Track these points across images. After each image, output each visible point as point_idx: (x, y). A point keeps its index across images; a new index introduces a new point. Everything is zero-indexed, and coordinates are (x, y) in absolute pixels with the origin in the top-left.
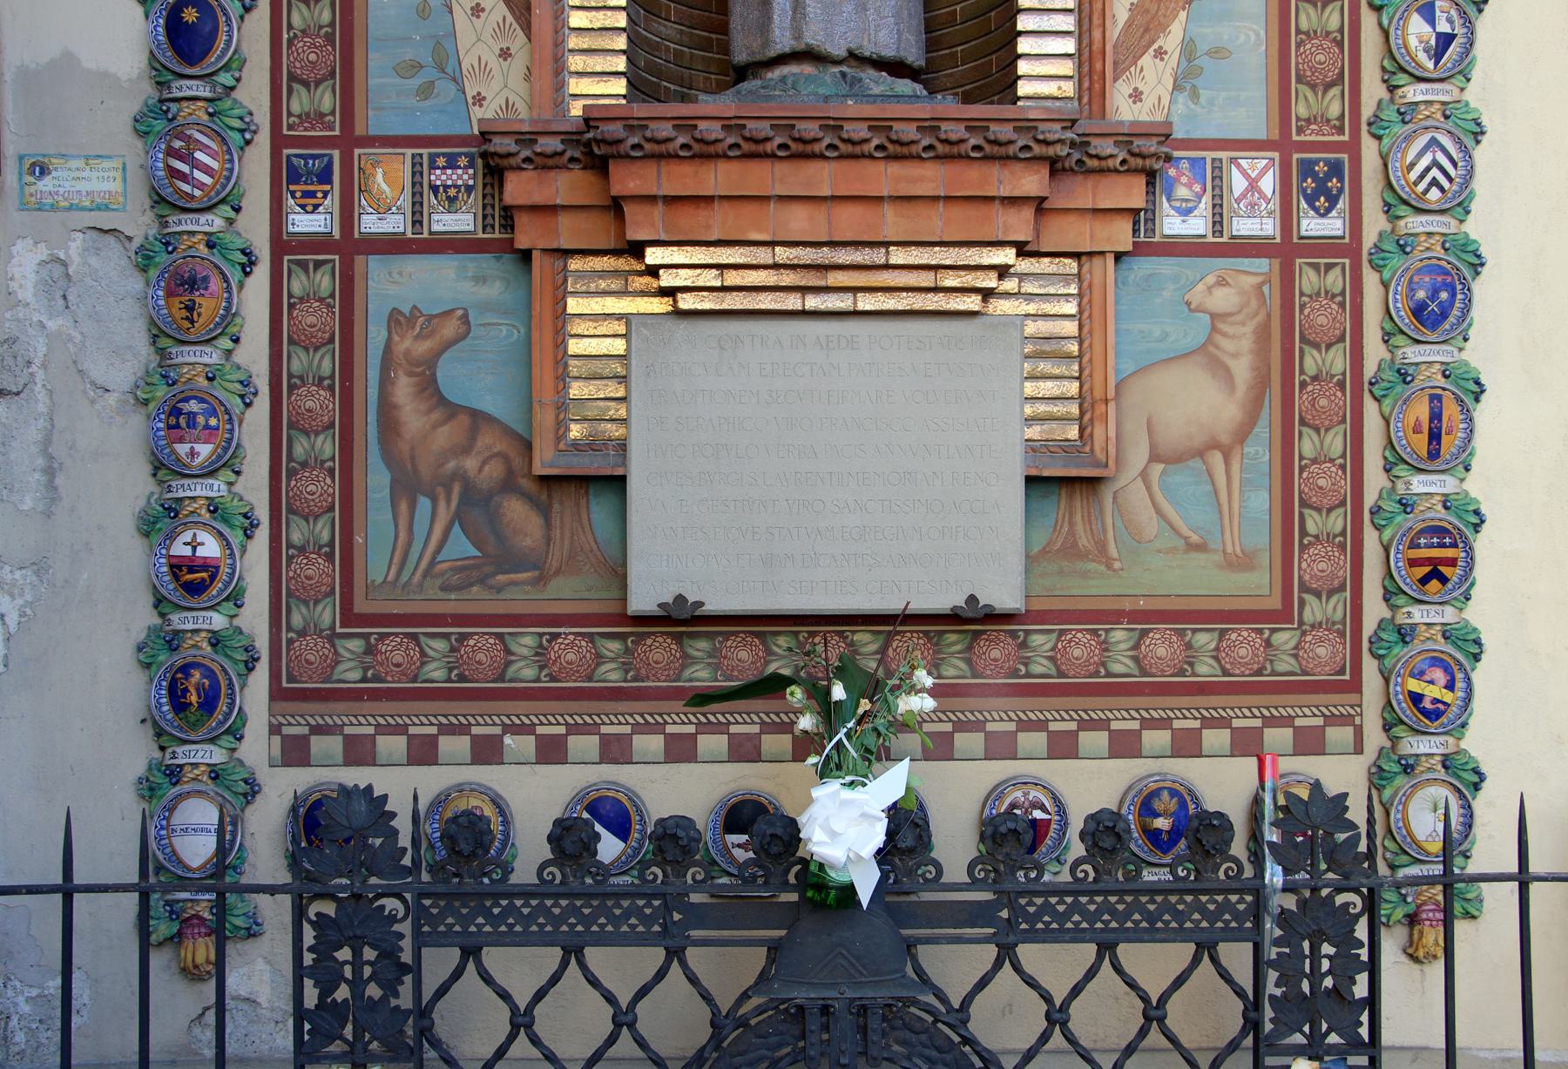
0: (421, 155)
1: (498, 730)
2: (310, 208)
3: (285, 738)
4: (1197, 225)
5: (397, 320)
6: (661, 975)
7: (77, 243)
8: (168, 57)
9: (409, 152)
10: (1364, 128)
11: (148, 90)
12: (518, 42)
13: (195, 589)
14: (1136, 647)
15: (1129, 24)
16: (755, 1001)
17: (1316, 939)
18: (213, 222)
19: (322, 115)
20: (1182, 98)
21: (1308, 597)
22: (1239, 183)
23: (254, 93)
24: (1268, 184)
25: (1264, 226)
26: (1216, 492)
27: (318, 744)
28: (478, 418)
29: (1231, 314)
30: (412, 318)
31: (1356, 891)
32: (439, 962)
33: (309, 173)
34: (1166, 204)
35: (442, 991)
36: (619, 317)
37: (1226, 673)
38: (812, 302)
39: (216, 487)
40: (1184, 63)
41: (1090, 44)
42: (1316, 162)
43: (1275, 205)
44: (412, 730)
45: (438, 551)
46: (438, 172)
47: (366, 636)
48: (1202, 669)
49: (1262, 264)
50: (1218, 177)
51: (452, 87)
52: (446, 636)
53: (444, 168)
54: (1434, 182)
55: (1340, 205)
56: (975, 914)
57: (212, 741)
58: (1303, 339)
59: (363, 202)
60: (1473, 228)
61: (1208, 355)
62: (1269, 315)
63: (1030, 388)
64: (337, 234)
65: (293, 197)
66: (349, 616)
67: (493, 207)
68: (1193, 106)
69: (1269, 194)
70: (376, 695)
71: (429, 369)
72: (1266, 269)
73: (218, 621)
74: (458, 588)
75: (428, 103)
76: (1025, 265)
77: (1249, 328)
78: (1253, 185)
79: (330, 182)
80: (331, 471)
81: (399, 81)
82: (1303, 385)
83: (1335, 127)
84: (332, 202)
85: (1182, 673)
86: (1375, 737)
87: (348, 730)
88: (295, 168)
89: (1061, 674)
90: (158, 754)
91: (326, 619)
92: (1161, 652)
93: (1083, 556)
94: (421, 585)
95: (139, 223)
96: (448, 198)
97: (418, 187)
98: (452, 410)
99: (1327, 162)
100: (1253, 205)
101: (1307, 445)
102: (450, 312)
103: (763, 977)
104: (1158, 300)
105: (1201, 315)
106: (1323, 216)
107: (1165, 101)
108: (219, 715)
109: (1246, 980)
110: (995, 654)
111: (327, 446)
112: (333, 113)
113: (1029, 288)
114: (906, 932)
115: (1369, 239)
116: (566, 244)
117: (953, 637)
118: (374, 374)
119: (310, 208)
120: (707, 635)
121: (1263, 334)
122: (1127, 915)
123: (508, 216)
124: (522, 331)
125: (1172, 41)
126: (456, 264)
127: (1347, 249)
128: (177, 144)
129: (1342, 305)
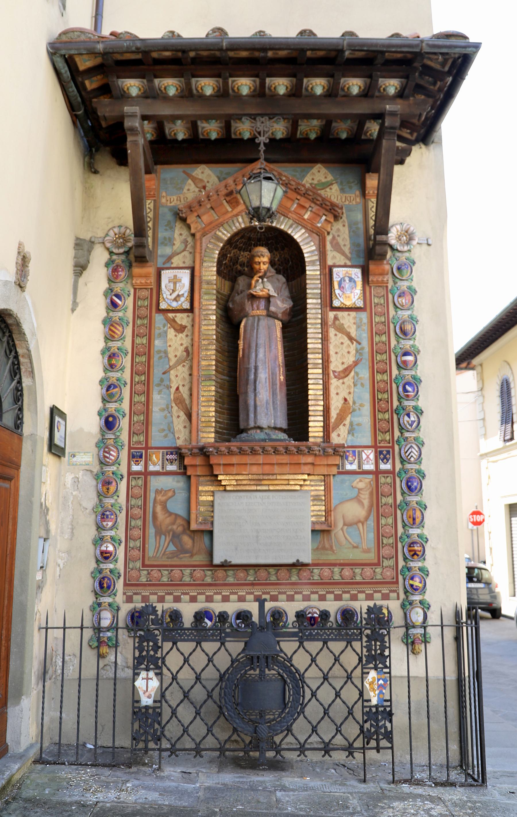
1: (180, 594)
3: (127, 596)
4: (354, 467)
5: (157, 492)
6: (219, 649)
7: (81, 473)
8: (104, 429)
9: (161, 451)
11: (99, 436)
12: (188, 425)
13: (106, 558)
14: (341, 572)
15: (336, 419)
16: (242, 655)
17: (376, 640)
18: (114, 468)
19: (140, 442)
20: (350, 436)
21: (384, 560)
23: (124, 437)
24: (372, 456)
26: (360, 533)
27: (135, 597)
28: (176, 515)
30: (161, 492)
31: (385, 629)
32: (167, 646)
35: (168, 653)
37: (364, 579)
38: (259, 488)
39: (112, 533)
44: (159, 594)
45: (166, 548)
47: (148, 570)
48: (357, 578)
52: (168, 570)
54: (412, 456)
56: (294, 635)
57: (109, 596)
60: (423, 467)
61: (357, 499)
62: (373, 489)
63: (313, 508)
64: (143, 471)
66: (144, 565)
70: (150, 585)
73: (111, 566)
74: (171, 558)
76: (311, 477)
77: (368, 492)
80: (140, 529)
84: (142, 463)
85: (352, 579)
86: (402, 596)
87: (143, 594)
89: (322, 579)
90: (95, 599)
91: (138, 566)
92: (347, 574)
93: (326, 549)
94: (162, 557)
95: (96, 469)
98: (171, 514)
101: (383, 521)
102: (170, 490)
103: (244, 650)
107: (346, 436)
108: (111, 590)
109: (359, 651)
110: (305, 574)
111: (140, 523)
113: (312, 483)
114: (277, 639)
115: (397, 470)
116: (198, 474)
117: (294, 570)
118: (151, 505)
120: (233, 570)
122: (330, 635)
123: (185, 468)
125: (347, 422)
127: (392, 472)
128: (106, 450)
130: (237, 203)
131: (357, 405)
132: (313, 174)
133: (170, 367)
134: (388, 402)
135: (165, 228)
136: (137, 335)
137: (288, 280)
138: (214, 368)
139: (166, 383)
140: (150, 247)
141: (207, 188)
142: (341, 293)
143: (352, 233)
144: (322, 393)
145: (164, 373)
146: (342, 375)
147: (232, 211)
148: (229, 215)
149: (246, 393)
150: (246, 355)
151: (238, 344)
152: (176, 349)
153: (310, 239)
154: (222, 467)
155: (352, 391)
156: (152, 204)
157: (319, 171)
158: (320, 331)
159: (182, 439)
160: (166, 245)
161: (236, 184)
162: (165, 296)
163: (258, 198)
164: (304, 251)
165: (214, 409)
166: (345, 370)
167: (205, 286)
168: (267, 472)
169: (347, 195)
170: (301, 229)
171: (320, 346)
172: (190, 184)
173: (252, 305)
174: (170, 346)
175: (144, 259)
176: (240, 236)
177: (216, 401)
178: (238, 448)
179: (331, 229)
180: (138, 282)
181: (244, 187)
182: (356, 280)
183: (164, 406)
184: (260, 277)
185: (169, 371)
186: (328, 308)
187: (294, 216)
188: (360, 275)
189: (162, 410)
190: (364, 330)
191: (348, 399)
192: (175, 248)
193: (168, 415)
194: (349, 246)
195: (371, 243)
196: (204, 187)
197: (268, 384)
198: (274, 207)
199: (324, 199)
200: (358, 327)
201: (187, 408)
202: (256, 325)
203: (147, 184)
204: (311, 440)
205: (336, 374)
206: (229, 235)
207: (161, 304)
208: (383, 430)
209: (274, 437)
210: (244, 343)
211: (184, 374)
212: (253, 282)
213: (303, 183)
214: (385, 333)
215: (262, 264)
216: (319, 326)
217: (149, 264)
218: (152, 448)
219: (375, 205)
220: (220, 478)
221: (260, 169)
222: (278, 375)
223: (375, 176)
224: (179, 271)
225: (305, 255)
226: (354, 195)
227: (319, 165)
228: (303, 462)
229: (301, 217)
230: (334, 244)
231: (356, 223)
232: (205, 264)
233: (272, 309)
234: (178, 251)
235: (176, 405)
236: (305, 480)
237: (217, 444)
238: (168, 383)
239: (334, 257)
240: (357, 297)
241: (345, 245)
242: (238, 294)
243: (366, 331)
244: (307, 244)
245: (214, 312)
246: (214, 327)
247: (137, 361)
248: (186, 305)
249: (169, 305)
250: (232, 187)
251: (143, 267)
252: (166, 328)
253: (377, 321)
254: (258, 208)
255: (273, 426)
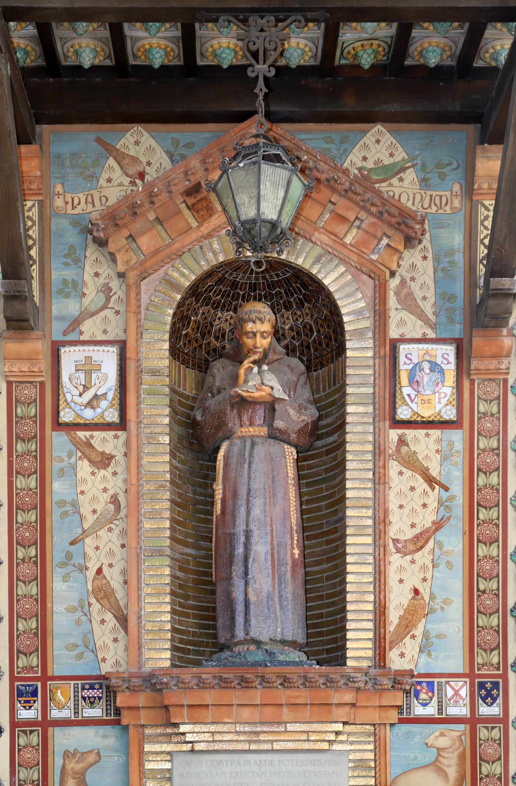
0: (78, 684)
2: (27, 708)
4: (431, 711)
5: (67, 754)
9: (72, 683)
10: (509, 668)
12: (121, 635)
15: (399, 625)
19: (33, 668)
20: (423, 656)
22: (450, 692)
24: (464, 692)
25: (463, 711)
29: (447, 749)
30: (74, 755)
33: (27, 693)
34: (416, 702)
36: (168, 753)
40: (424, 640)
41: (380, 634)
42: (486, 683)
43: (467, 701)
46: (86, 691)
49: (461, 727)
50: (440, 690)
51: (92, 655)
53: (88, 689)
55: (498, 701)
58: (481, 759)
59: (52, 704)
64: (40, 718)
65: (20, 703)
67: (110, 705)
68: (428, 659)
69: (464, 697)
71: (82, 775)
72: (463, 729)
75: (81, 661)
78: (456, 693)
79: (36, 696)
81: (66, 652)
82: (481, 779)
83: (495, 667)
84: (38, 705)
88: (21, 691)
96: (90, 702)
97: (76, 698)
99: (491, 683)
100: (456, 702)
104: (412, 743)
105: (432, 749)
106: (489, 706)
107: (416, 657)
112: (38, 666)
113: (351, 739)
116: (142, 722)
119: (27, 708)
121: (462, 757)
124: (124, 758)
125: (418, 631)
126: (94, 730)
129: (499, 744)
130: (210, 211)
131: (438, 601)
132: (366, 147)
133: (84, 531)
134: (497, 595)
135: (65, 260)
136: (18, 473)
137: (308, 368)
138: (168, 533)
139: (78, 560)
140: (37, 299)
141: (147, 178)
142: (413, 394)
143: (440, 274)
144: (371, 579)
145: (72, 543)
146: (411, 547)
147: (199, 227)
148: (194, 235)
149: (229, 578)
150: (228, 511)
151: (214, 491)
152: (94, 498)
153: (355, 286)
154: (185, 710)
155: (429, 576)
156: (35, 210)
157: (378, 141)
158: (370, 465)
159: (111, 661)
160: (67, 296)
161: (206, 170)
162: (69, 397)
163: (254, 201)
164: (343, 311)
165: (168, 608)
166: (417, 537)
167: (146, 378)
168: (268, 720)
169: (434, 193)
170: (337, 266)
171: (370, 494)
172: (111, 168)
173: (240, 417)
174: (82, 493)
175: (24, 324)
176: (216, 278)
177: (173, 593)
178: (215, 677)
179: (399, 266)
180: (15, 369)
181: (225, 176)
182: (444, 367)
183: (76, 604)
184: (254, 362)
185: (83, 539)
186: (387, 423)
187: (324, 238)
188: (452, 358)
189: (72, 610)
190: (456, 464)
191: (421, 590)
192: (86, 301)
193: (84, 618)
194: (433, 300)
195: (479, 292)
196: (142, 176)
197: (269, 563)
198: (286, 221)
199: (385, 202)
200: (445, 458)
201: (119, 607)
202: (247, 454)
203: (26, 166)
204: (350, 663)
205: (400, 546)
206: (194, 278)
207: (62, 414)
208: (487, 647)
209: (281, 658)
210: (224, 489)
211: (110, 545)
212: (242, 372)
213: (345, 165)
214: (498, 469)
215: (258, 335)
216: (369, 457)
217: (35, 334)
218: (54, 678)
219: (491, 214)
220: (183, 729)
221: (256, 136)
222: (289, 547)
223: (496, 150)
224: (96, 348)
225: (345, 319)
226: (448, 193)
227: (379, 127)
228: (335, 701)
229: (339, 239)
230: (403, 295)
231: (451, 252)
232: (146, 337)
233: (279, 424)
234: (93, 309)
235: (98, 601)
236: (337, 733)
237: (175, 671)
238: (82, 561)
239: (402, 322)
240: (444, 401)
241: (424, 298)
242: (213, 396)
243: (460, 466)
244: (347, 296)
245: (167, 430)
246: (167, 458)
247: (20, 520)
248: (113, 416)
249: (78, 415)
250: (199, 176)
251: (23, 339)
252: (73, 459)
253: (482, 446)
254: (253, 221)
255: (279, 637)
